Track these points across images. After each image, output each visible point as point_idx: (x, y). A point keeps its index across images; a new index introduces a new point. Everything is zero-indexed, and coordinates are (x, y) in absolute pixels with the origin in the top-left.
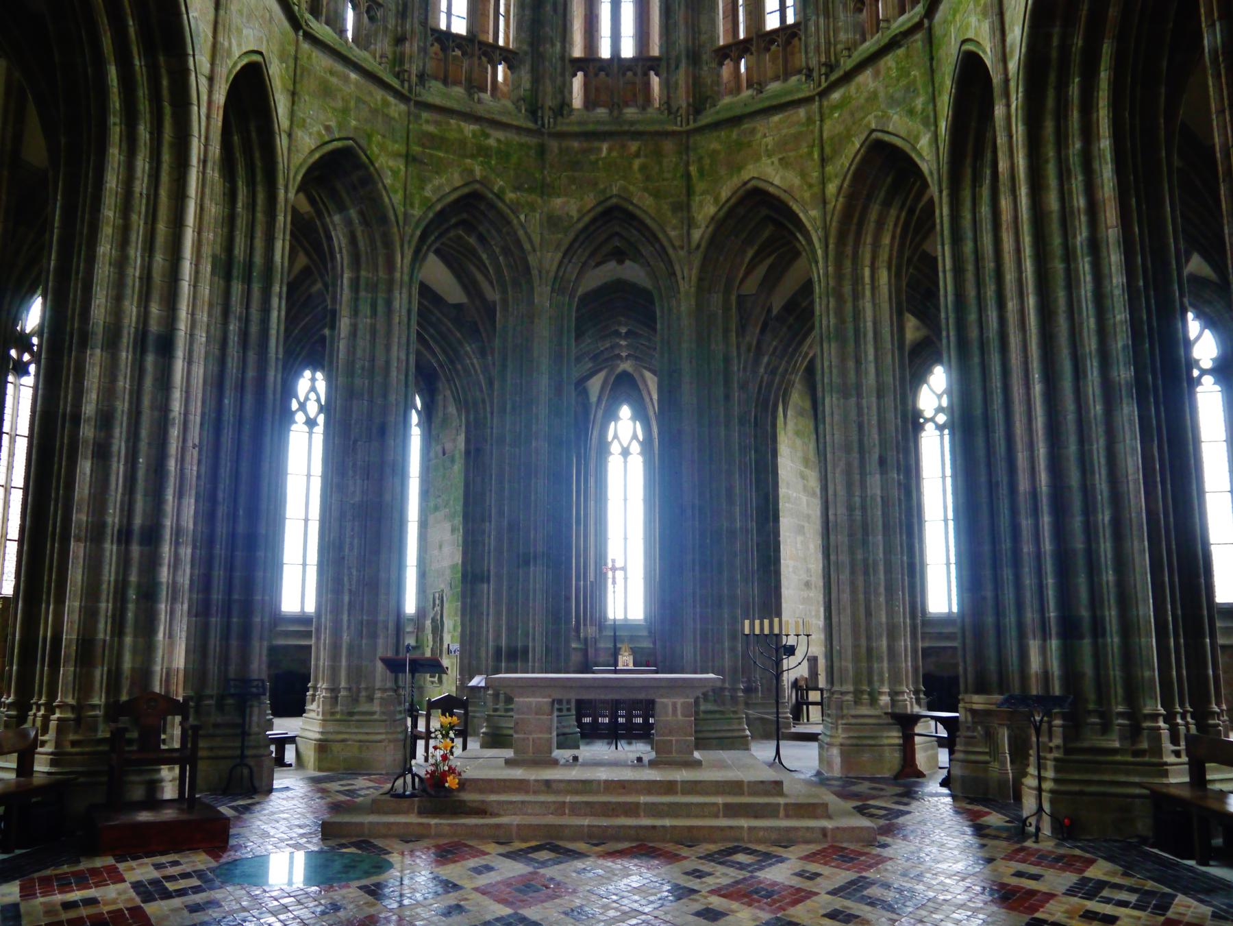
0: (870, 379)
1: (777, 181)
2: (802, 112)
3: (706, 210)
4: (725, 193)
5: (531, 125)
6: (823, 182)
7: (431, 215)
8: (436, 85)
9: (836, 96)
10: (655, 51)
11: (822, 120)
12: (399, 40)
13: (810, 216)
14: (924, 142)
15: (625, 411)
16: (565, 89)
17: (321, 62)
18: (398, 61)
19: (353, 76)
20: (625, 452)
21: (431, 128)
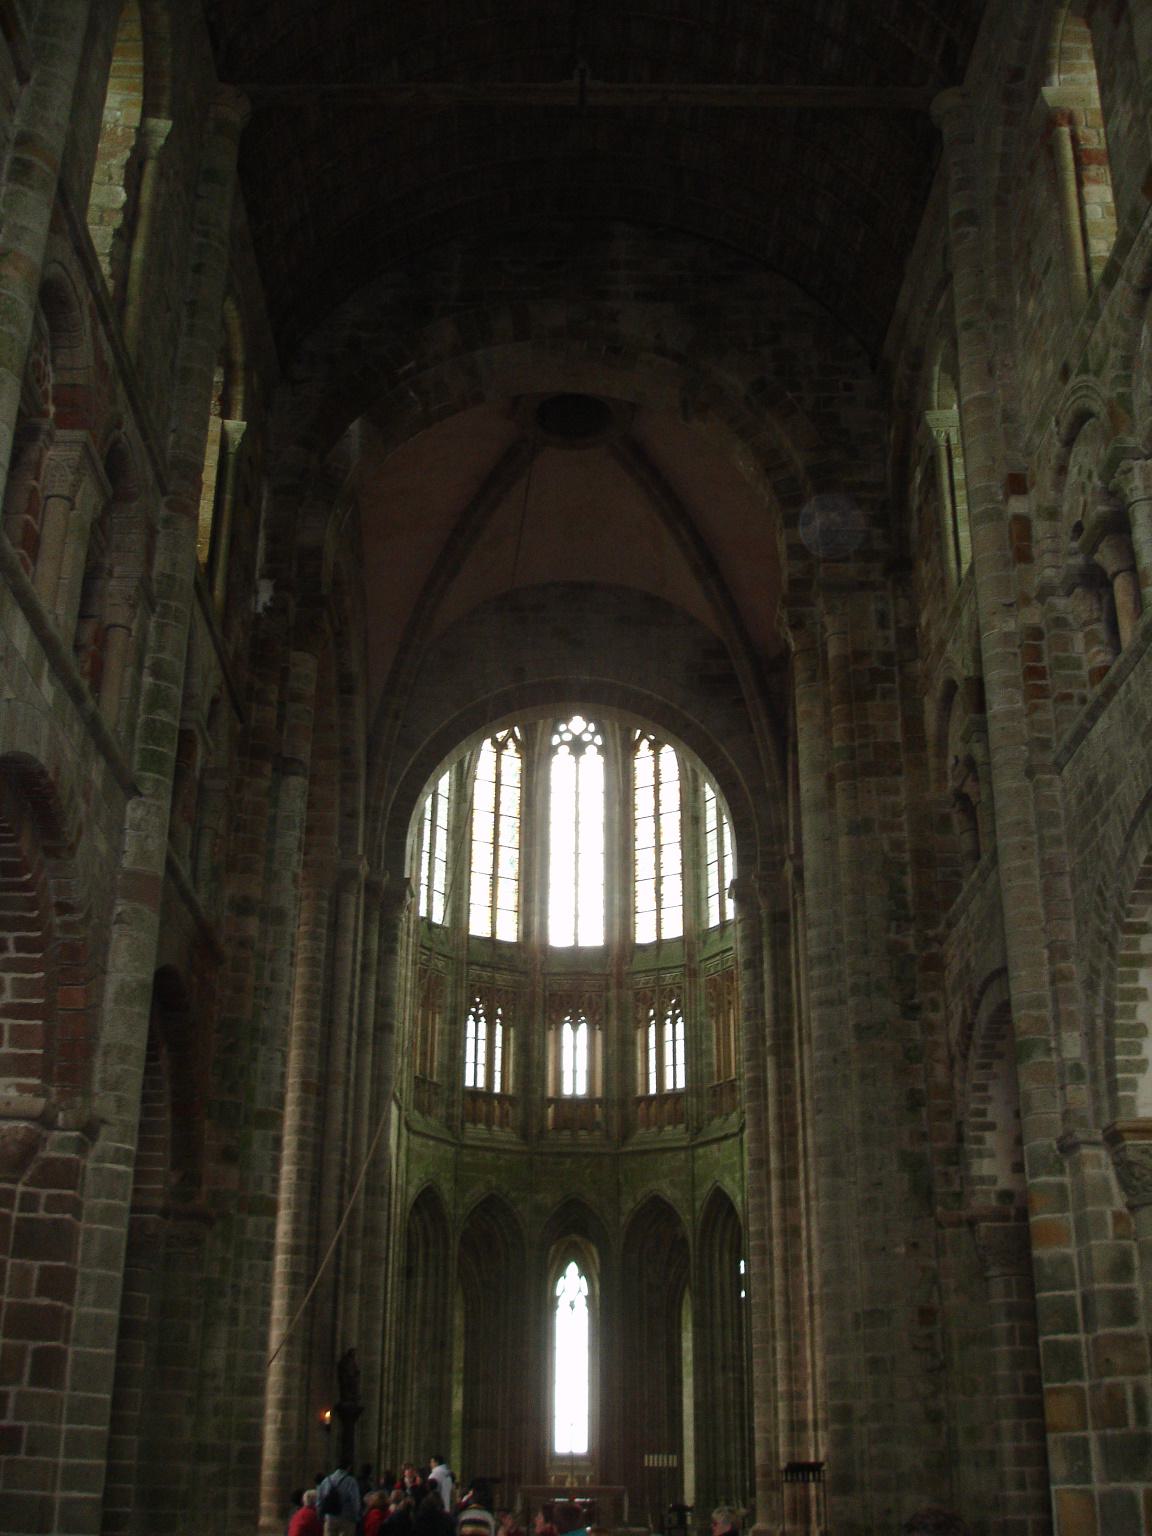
0: (718, 1319)
1: (669, 1193)
2: (682, 1155)
3: (629, 1205)
4: (639, 1197)
5: (525, 1148)
6: (694, 1200)
7: (468, 1212)
8: (468, 1125)
9: (701, 1151)
10: (599, 1093)
11: (693, 1162)
12: (451, 1104)
13: (686, 1218)
14: (739, 1199)
15: (572, 1269)
16: (543, 1117)
17: (417, 1141)
18: (450, 1118)
19: (431, 1143)
20: (572, 1306)
21: (468, 1159)
